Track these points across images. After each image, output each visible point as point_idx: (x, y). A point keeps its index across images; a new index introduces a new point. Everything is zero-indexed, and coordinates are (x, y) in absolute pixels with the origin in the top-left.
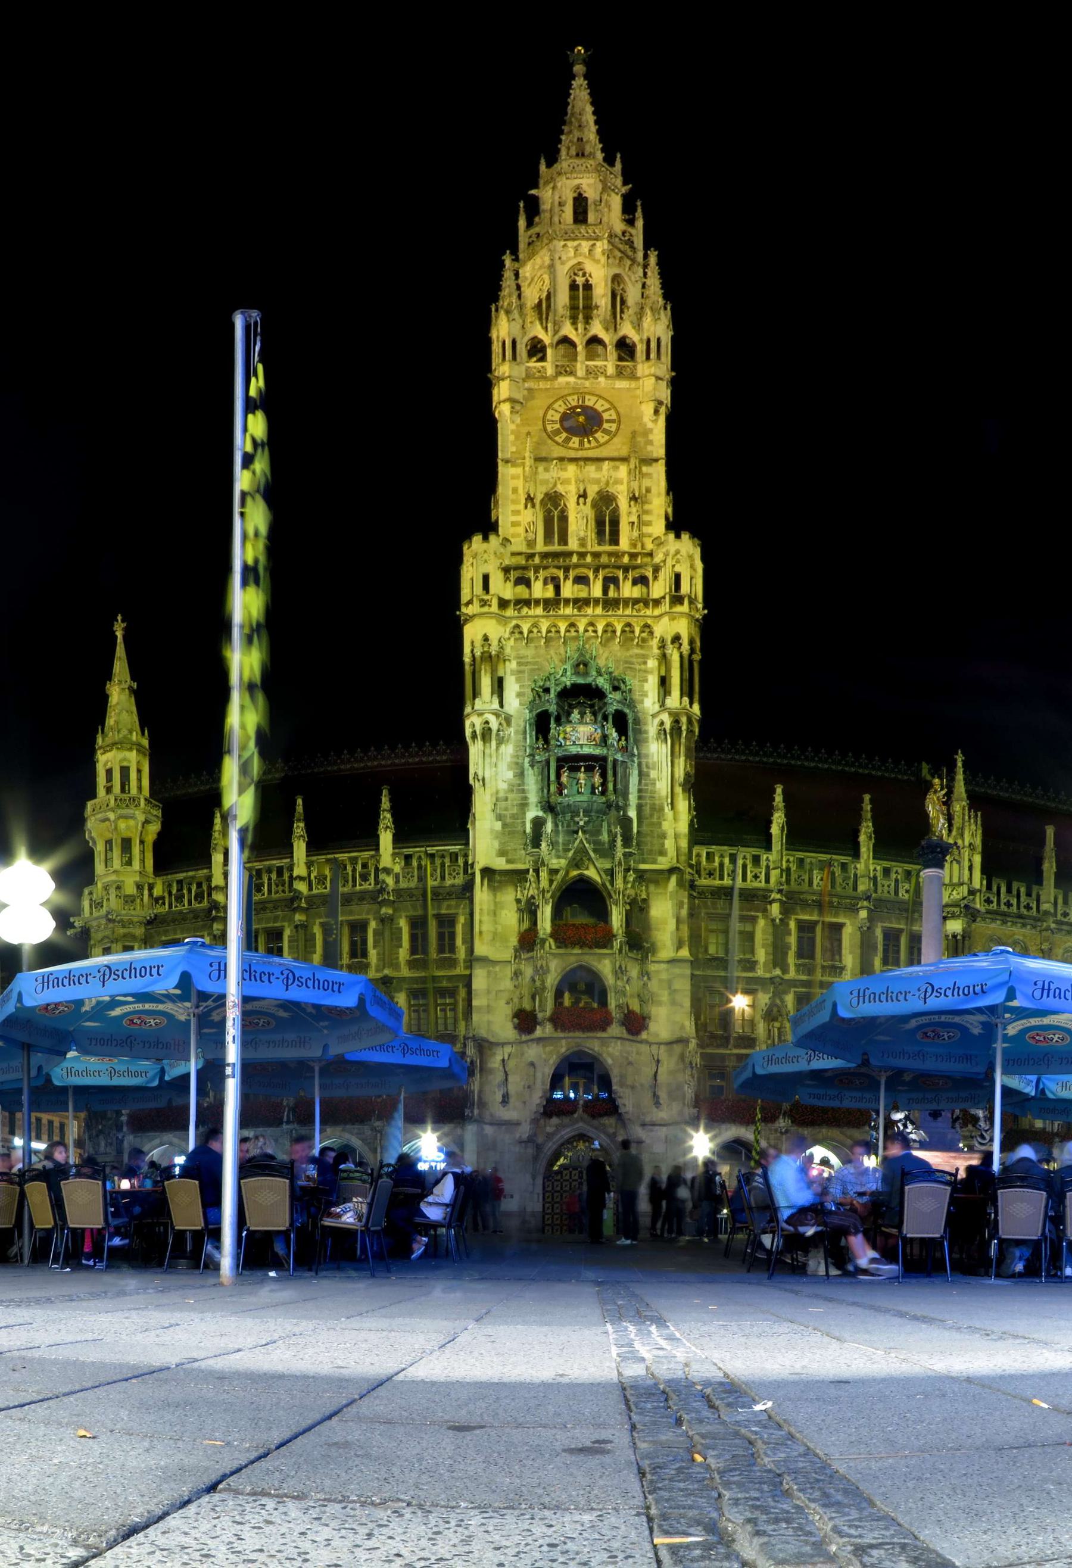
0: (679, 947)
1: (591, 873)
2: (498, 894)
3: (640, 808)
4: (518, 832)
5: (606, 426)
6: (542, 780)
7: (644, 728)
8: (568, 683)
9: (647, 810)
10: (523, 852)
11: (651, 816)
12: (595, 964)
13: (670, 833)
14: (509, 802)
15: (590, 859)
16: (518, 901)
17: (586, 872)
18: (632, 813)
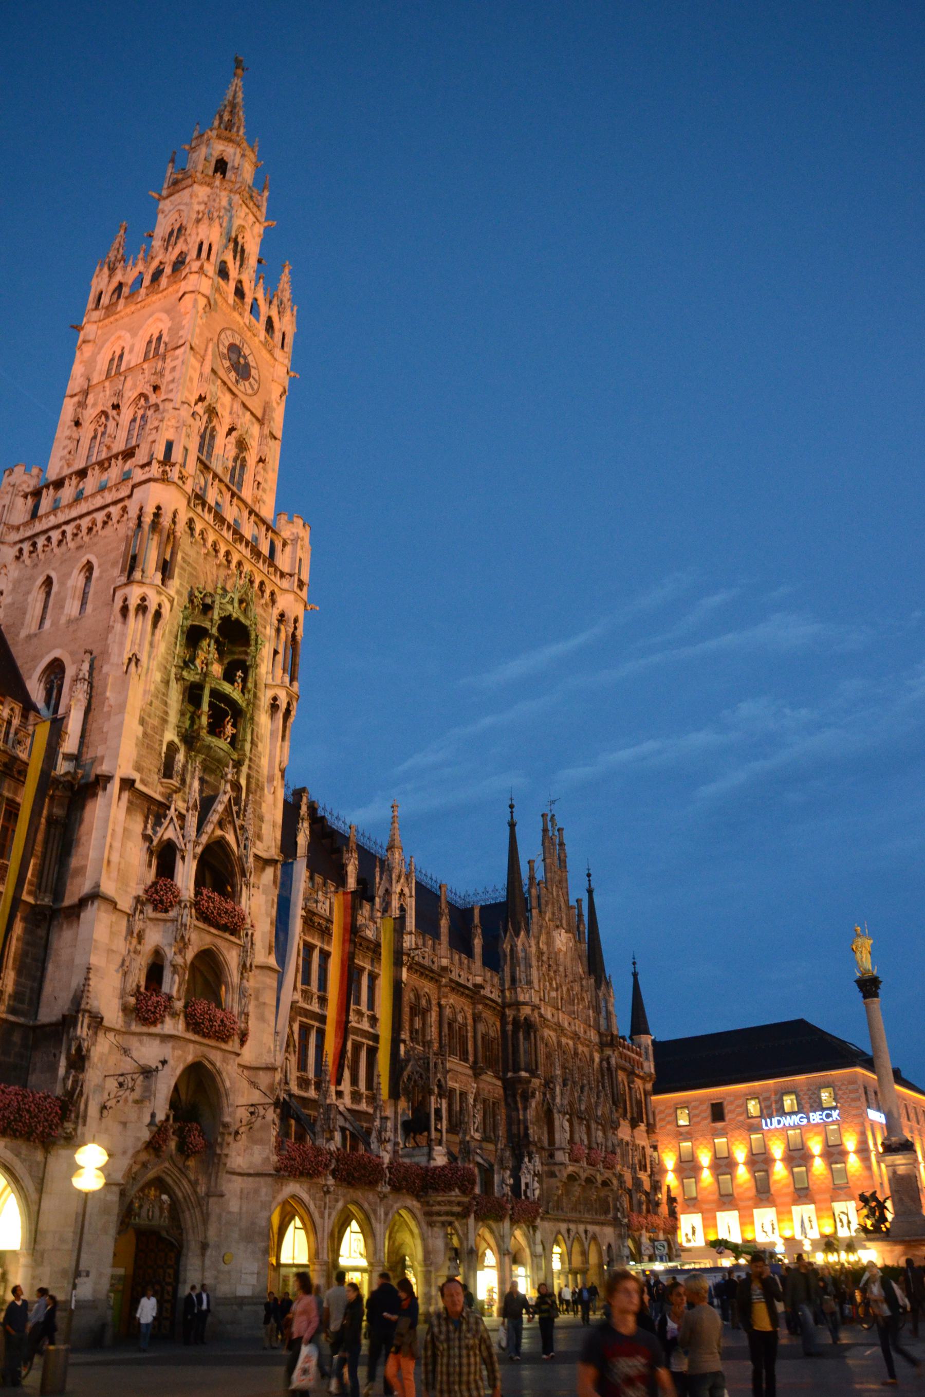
0: (270, 953)
1: (230, 838)
2: (128, 817)
3: (249, 777)
4: (155, 750)
5: (251, 380)
6: (183, 700)
7: (260, 694)
8: (235, 615)
9: (253, 786)
10: (156, 777)
11: (256, 791)
12: (225, 952)
13: (267, 817)
14: (153, 709)
15: (232, 822)
16: (147, 838)
17: (227, 836)
18: (243, 782)
